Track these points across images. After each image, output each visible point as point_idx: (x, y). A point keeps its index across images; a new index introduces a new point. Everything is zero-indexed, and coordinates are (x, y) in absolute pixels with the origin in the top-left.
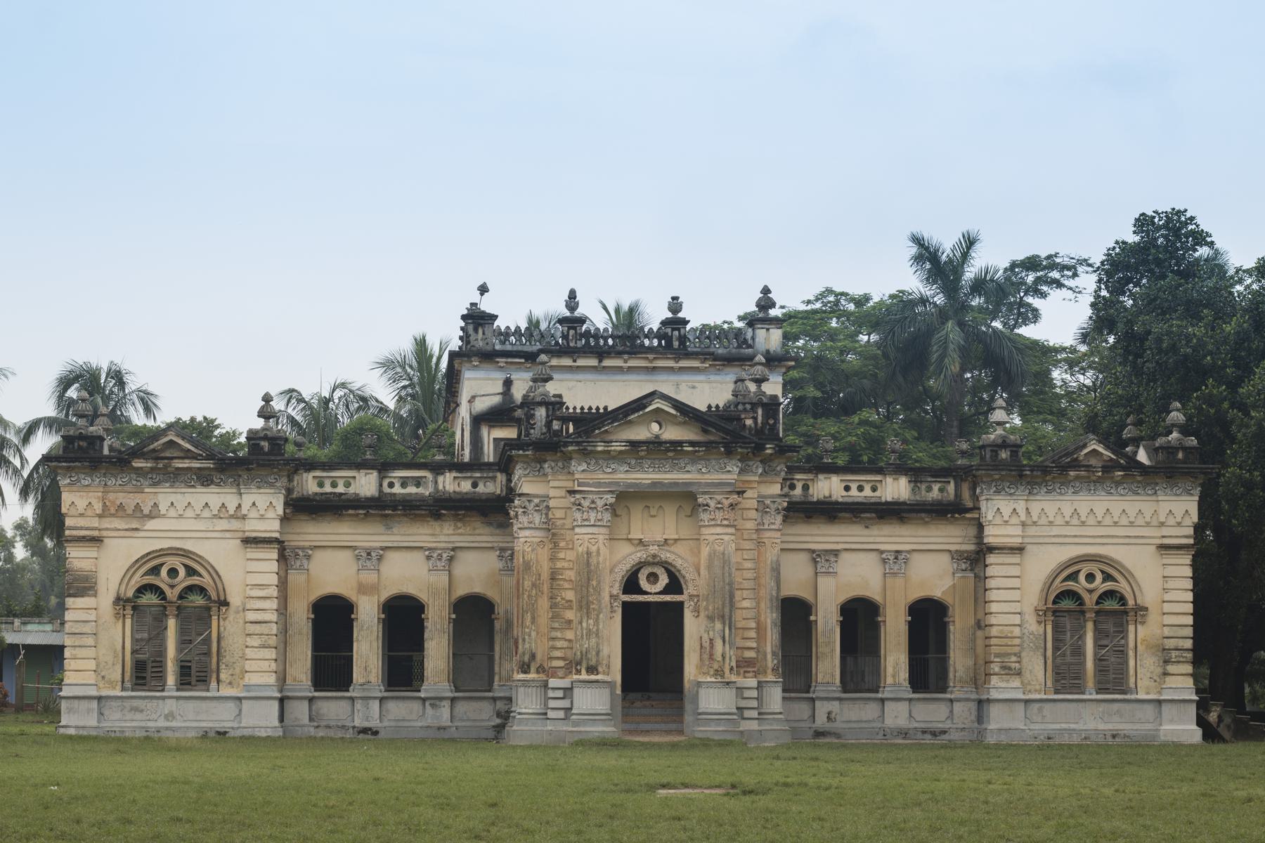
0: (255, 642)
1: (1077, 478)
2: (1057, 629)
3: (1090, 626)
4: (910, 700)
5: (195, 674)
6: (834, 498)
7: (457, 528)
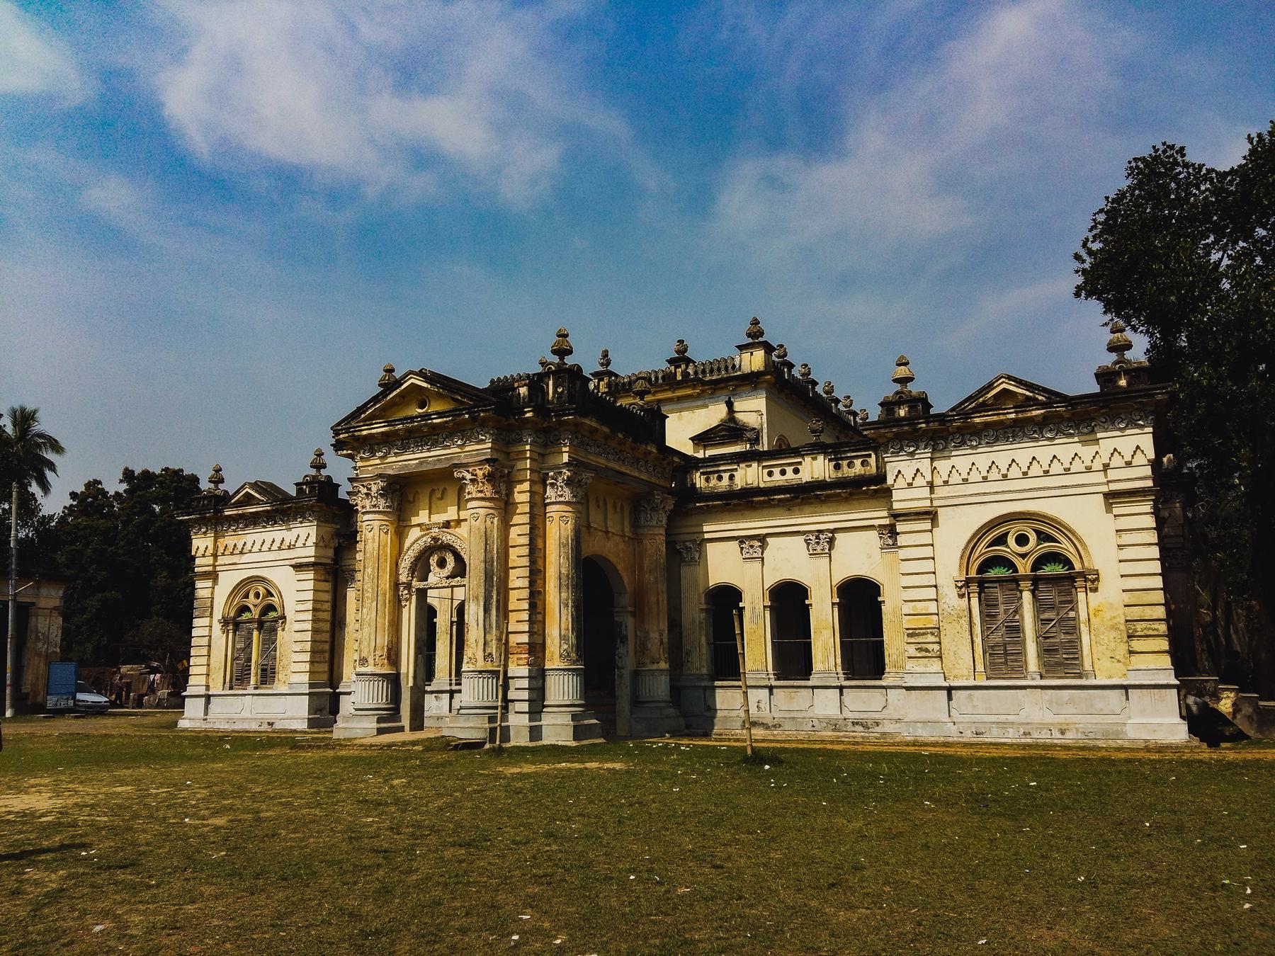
0: (298, 647)
1: (987, 425)
2: (988, 606)
3: (1027, 596)
4: (841, 688)
5: (268, 675)
6: (755, 485)
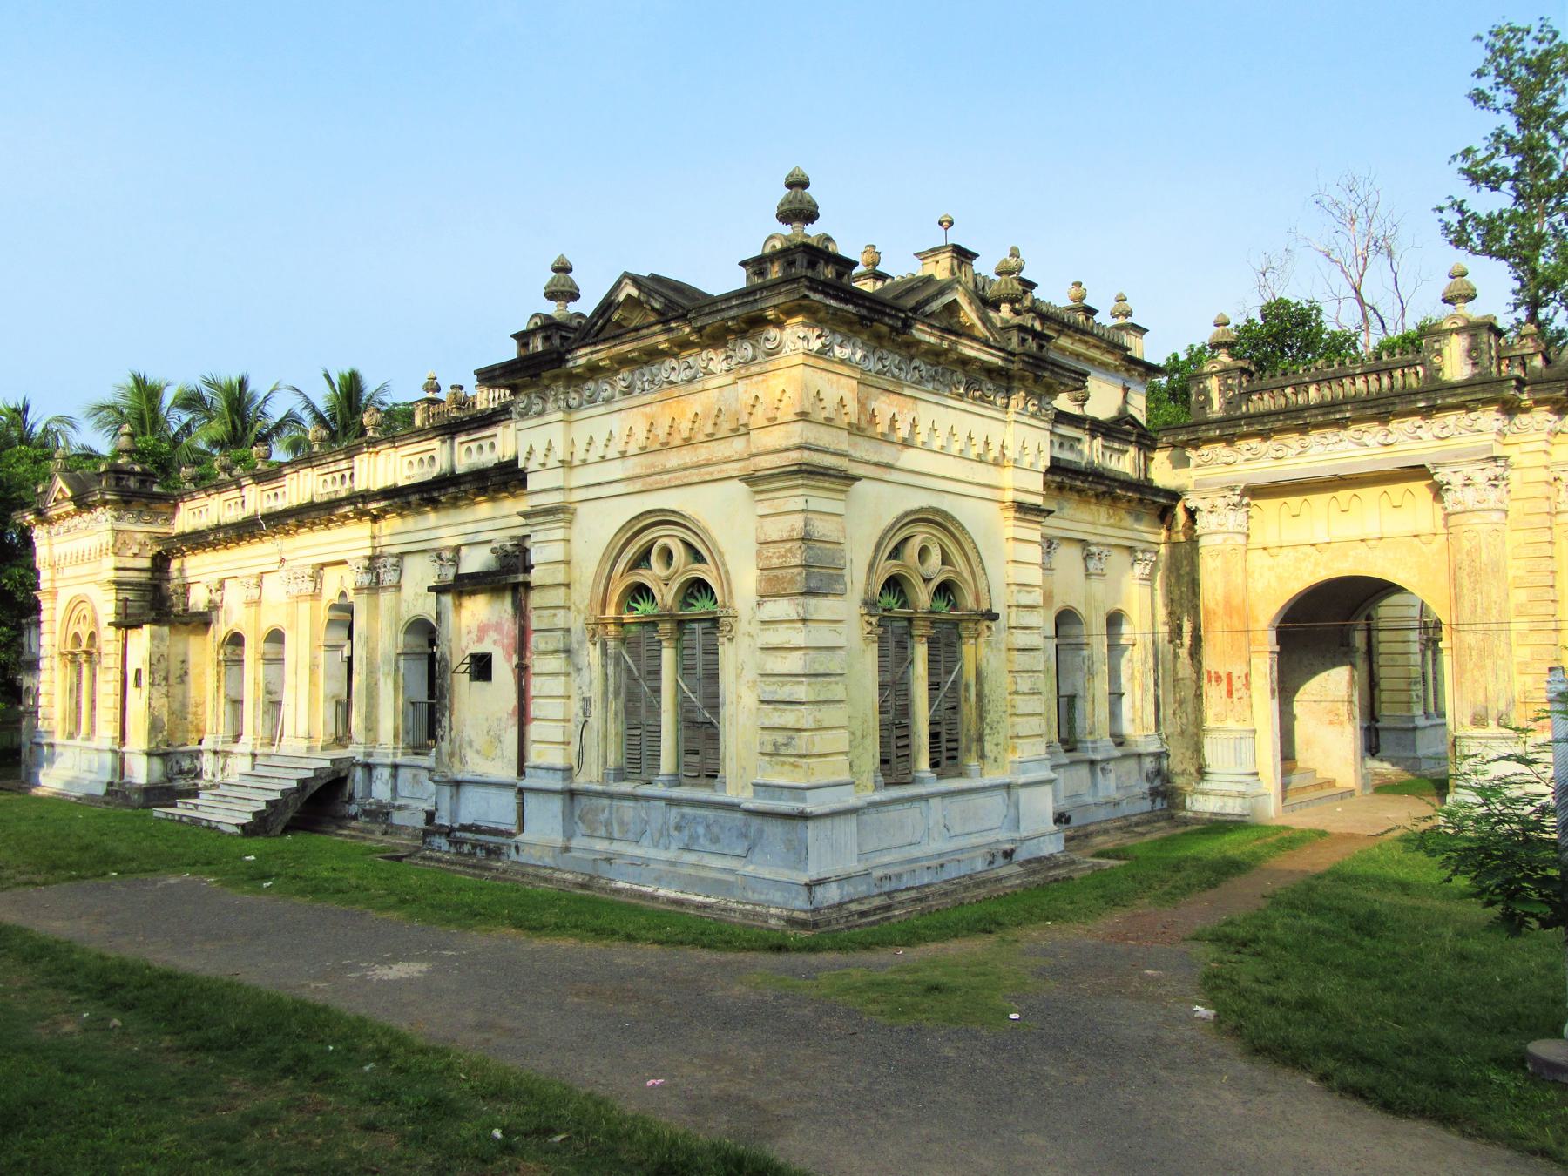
0: (1024, 684)
7: (1110, 517)
